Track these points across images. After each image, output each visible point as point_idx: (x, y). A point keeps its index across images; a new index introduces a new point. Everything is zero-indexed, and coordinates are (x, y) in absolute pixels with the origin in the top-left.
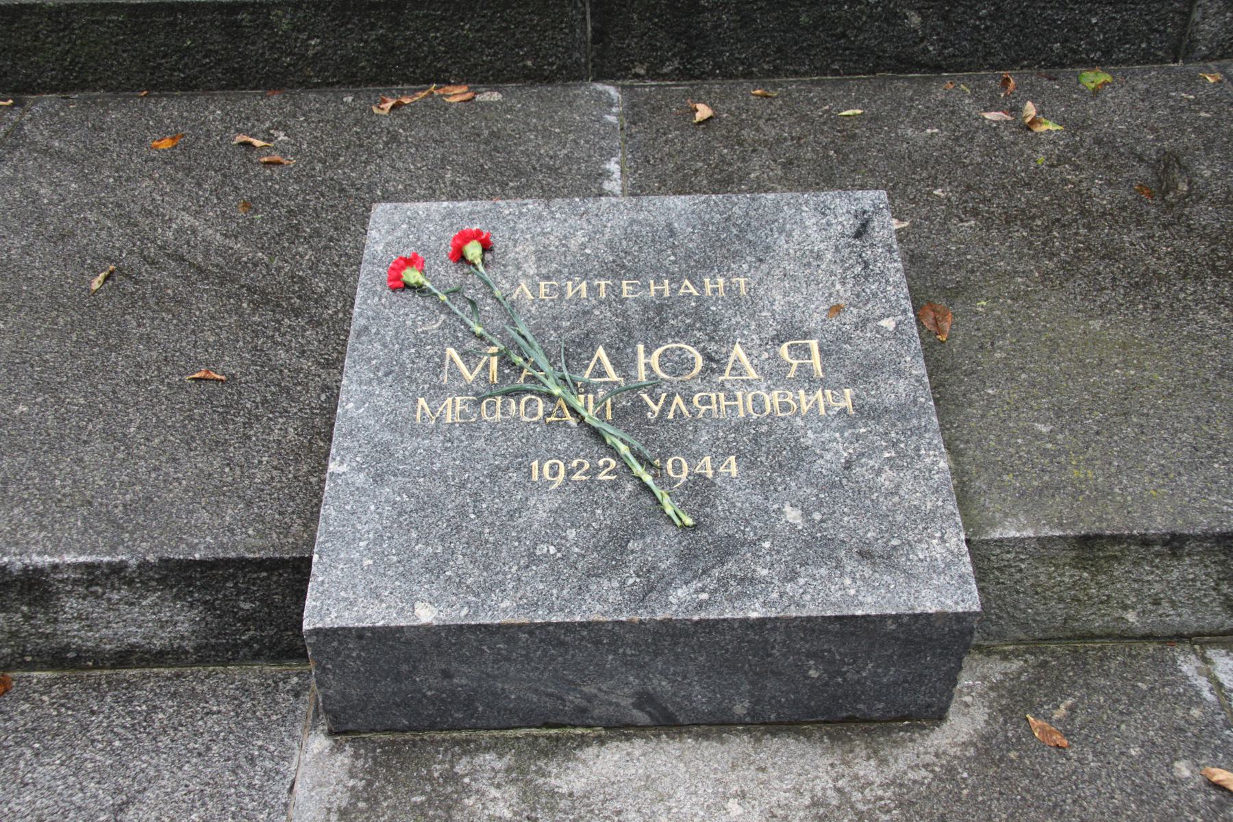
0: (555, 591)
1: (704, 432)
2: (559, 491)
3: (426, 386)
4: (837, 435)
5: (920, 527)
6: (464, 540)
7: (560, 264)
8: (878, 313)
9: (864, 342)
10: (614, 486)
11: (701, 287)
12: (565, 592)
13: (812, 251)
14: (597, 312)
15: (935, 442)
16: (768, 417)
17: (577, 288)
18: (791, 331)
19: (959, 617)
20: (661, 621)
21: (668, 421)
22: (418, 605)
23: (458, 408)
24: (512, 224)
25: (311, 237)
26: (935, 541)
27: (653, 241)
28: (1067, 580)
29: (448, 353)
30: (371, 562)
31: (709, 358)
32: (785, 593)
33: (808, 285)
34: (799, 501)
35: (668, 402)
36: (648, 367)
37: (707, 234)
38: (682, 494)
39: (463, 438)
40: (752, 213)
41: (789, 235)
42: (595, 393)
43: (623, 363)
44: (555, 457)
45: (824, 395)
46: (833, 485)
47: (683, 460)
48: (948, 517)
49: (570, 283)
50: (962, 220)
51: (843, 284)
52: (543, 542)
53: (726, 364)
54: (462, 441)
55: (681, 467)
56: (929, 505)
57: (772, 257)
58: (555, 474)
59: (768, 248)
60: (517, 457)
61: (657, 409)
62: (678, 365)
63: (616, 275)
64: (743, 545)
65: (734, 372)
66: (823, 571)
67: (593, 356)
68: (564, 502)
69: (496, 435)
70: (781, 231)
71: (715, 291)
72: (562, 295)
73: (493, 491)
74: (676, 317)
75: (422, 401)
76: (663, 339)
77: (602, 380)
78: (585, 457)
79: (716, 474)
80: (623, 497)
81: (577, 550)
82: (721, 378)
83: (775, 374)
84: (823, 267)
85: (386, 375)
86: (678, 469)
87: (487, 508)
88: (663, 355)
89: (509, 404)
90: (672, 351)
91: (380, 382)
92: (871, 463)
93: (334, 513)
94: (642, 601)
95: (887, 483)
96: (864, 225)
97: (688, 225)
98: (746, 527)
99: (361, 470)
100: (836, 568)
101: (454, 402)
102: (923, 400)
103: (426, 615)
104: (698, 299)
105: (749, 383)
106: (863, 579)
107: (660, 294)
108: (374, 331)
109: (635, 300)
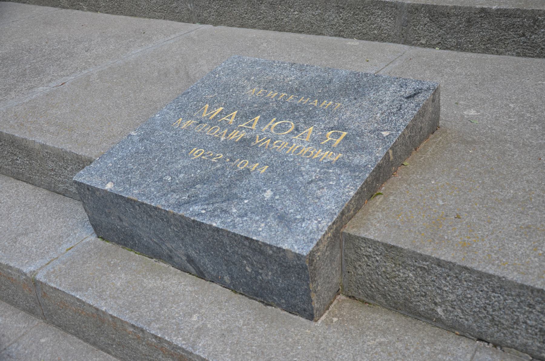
19: (298, 256)
20: (180, 216)
28: (402, 275)
66: (257, 218)
90: (286, 123)
103: (109, 186)
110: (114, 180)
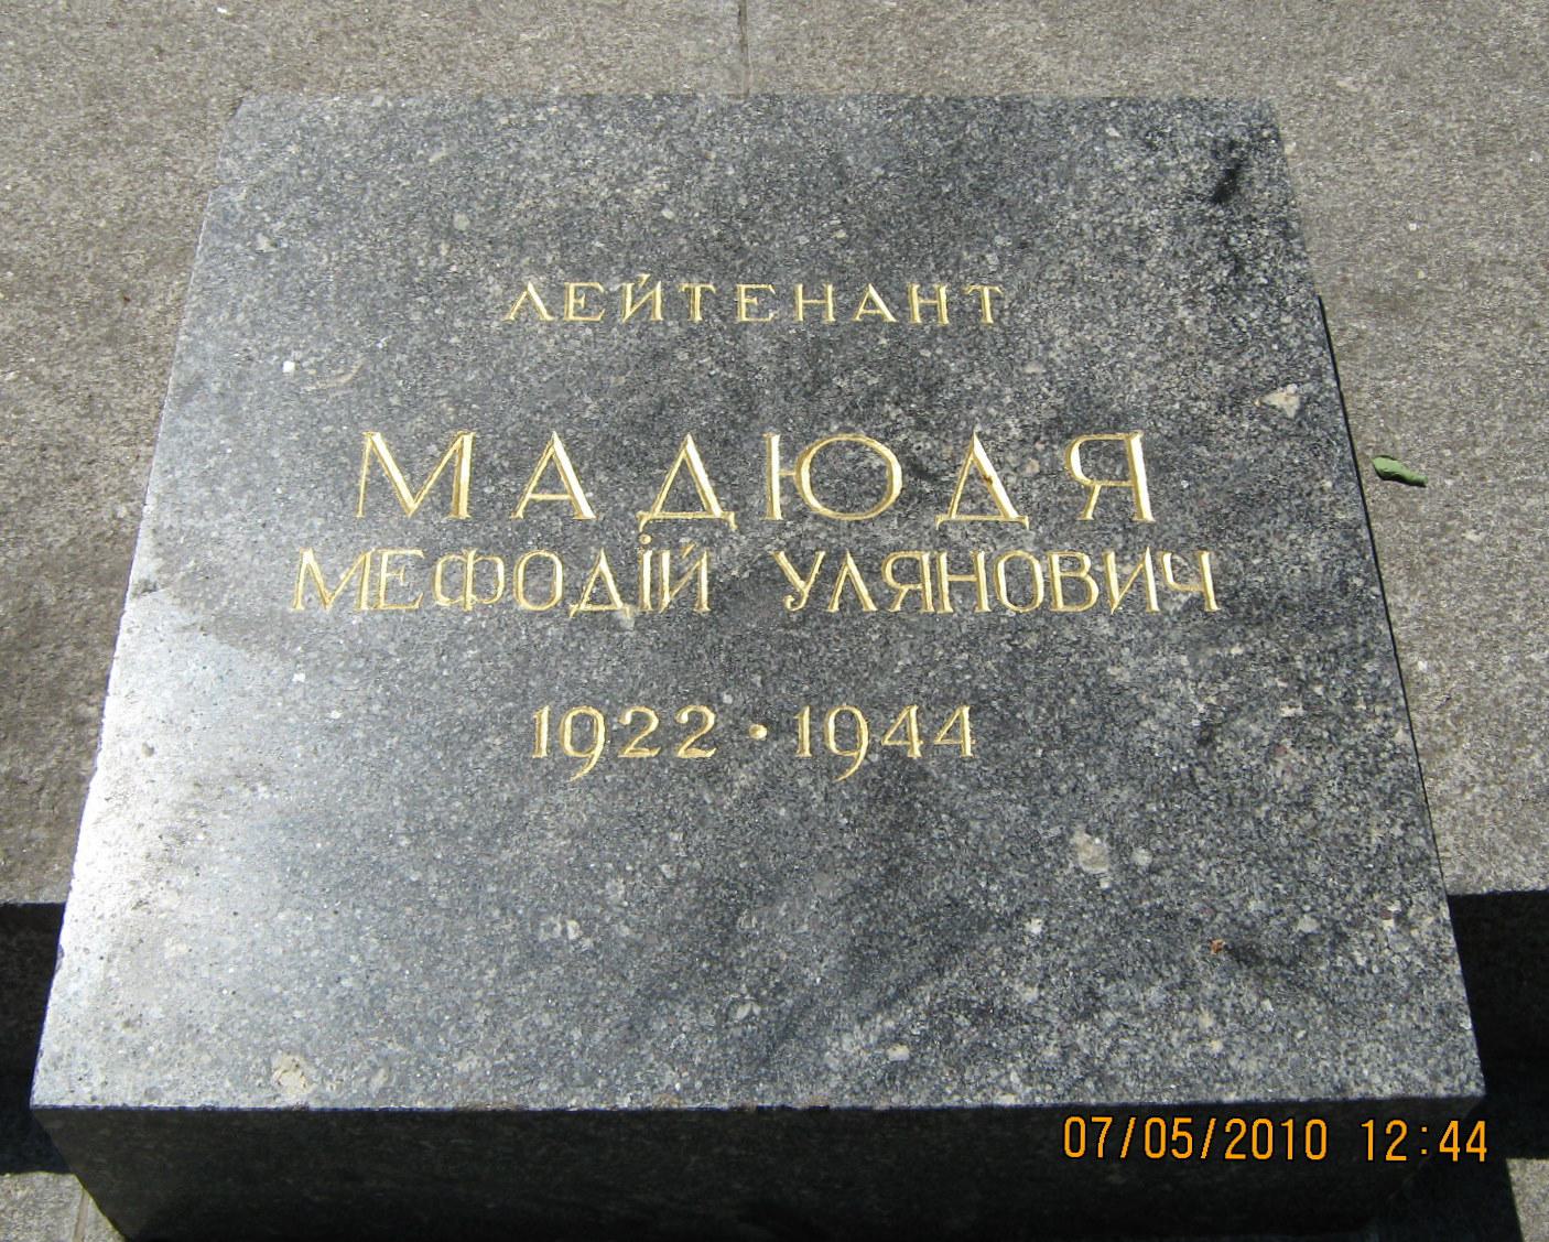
0: (577, 1034)
4: (1184, 660)
5: (1357, 888)
7: (609, 240)
8: (1264, 375)
9: (1236, 446)
10: (710, 773)
11: (901, 306)
12: (598, 1036)
14: (683, 356)
15: (1386, 682)
16: (1038, 613)
17: (640, 297)
18: (1084, 415)
21: (828, 618)
23: (384, 576)
26: (1389, 924)
29: (368, 445)
31: (914, 469)
33: (1121, 306)
34: (1104, 819)
35: (829, 575)
36: (789, 487)
39: (391, 649)
40: (1005, 138)
41: (1082, 190)
42: (675, 547)
43: (738, 483)
45: (1157, 567)
47: (857, 713)
48: (1415, 862)
50: (1393, 147)
51: (1192, 304)
52: (553, 910)
53: (952, 484)
54: (387, 657)
55: (854, 731)
56: (1376, 834)
58: (584, 743)
60: (503, 699)
62: (849, 484)
64: (983, 927)
65: (967, 506)
66: (1155, 995)
67: (671, 460)
71: (929, 312)
75: (308, 557)
76: (819, 420)
77: (690, 516)
78: (648, 703)
81: (626, 931)
82: (941, 518)
83: (1055, 514)
84: (1151, 264)
86: (847, 736)
88: (820, 460)
90: (839, 449)
92: (1255, 729)
94: (765, 1061)
95: (1288, 779)
96: (1233, 174)
97: (874, 162)
98: (990, 881)
100: (1182, 986)
102: (1359, 582)
105: (1000, 531)
106: (1241, 1016)
107: (815, 314)
108: (215, 388)
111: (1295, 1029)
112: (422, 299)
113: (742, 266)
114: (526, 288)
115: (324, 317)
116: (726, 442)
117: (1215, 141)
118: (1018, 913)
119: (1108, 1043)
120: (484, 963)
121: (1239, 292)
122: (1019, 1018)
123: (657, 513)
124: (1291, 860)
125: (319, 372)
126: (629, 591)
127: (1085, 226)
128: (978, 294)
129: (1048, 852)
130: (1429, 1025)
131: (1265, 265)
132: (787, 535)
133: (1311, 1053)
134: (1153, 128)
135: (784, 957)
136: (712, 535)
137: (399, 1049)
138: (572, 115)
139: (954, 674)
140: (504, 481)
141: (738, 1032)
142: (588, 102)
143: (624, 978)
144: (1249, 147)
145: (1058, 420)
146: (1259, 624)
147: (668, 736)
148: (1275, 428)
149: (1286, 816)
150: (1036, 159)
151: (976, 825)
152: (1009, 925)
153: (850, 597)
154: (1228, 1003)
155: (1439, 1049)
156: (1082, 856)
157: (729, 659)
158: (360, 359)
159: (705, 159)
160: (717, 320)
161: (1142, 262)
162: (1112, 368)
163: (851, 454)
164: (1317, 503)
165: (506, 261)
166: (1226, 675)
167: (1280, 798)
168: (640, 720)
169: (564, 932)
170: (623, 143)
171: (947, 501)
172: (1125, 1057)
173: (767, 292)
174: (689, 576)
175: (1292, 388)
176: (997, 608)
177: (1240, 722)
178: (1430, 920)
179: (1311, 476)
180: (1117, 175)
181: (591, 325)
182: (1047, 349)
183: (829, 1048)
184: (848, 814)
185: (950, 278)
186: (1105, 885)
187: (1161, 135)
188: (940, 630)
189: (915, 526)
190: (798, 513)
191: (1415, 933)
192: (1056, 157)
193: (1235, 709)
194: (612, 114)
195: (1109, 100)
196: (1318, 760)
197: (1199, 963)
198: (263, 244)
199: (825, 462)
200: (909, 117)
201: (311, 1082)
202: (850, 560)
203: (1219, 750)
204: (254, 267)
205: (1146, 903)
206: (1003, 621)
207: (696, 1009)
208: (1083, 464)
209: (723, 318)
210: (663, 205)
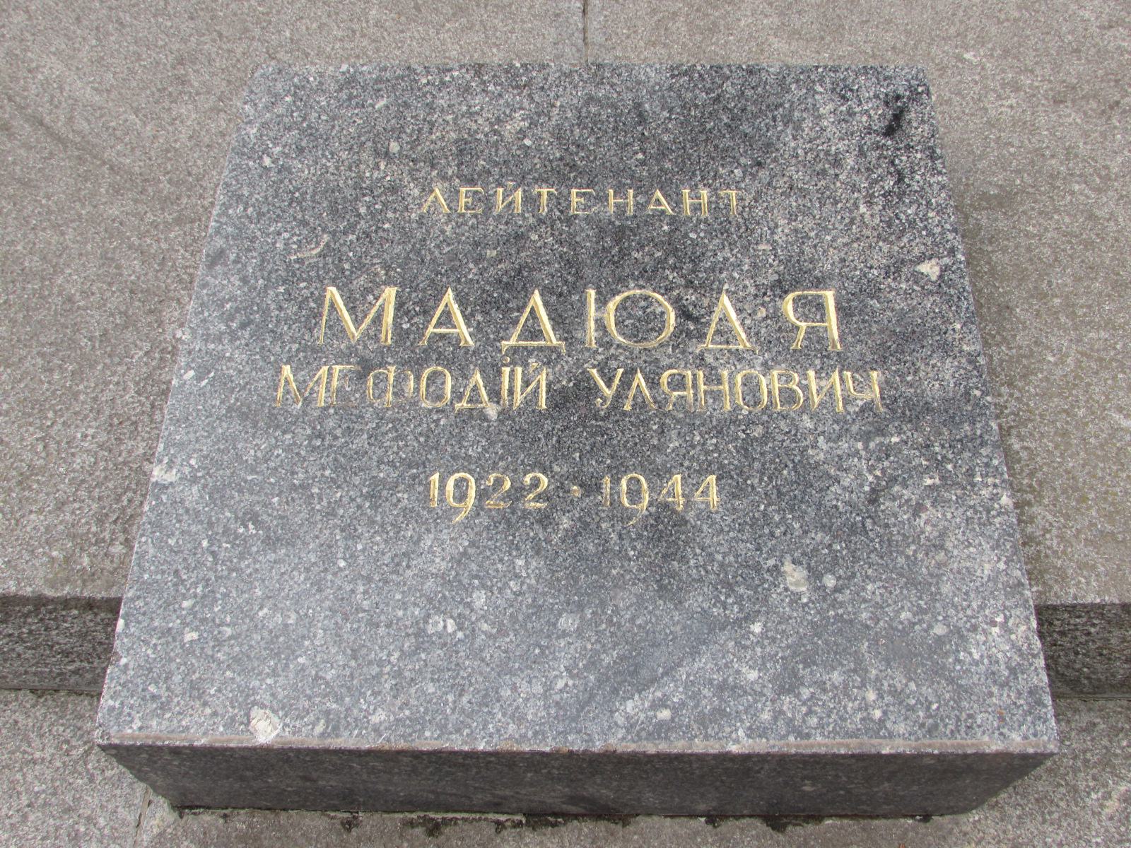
1: (674, 434)
2: (466, 526)
3: (295, 347)
4: (860, 445)
5: (974, 605)
6: (328, 603)
7: (489, 160)
8: (916, 252)
10: (545, 519)
11: (678, 203)
12: (465, 699)
13: (827, 153)
14: (534, 237)
15: (995, 462)
16: (764, 411)
17: (508, 198)
18: (796, 276)
21: (624, 414)
22: (256, 712)
23: (335, 383)
24: (429, 99)
25: (198, 94)
26: (996, 630)
27: (615, 129)
29: (328, 296)
30: (195, 635)
31: (684, 314)
32: (782, 712)
33: (822, 205)
36: (601, 325)
37: (688, 122)
38: (640, 536)
39: (338, 432)
40: (749, 93)
41: (798, 127)
42: (525, 365)
43: (566, 320)
44: (464, 469)
45: (842, 380)
46: (853, 530)
47: (642, 479)
49: (500, 190)
50: (999, 97)
51: (870, 204)
52: (439, 611)
53: (708, 324)
54: (336, 438)
55: (639, 492)
56: (987, 566)
57: (775, 160)
58: (461, 497)
59: (769, 145)
60: (410, 467)
61: (609, 392)
62: (640, 323)
63: (563, 180)
64: (723, 629)
65: (718, 338)
66: (837, 677)
67: (525, 306)
68: (473, 544)
69: (384, 429)
70: (787, 120)
71: (697, 208)
72: (489, 208)
73: (372, 522)
74: (642, 247)
75: (287, 370)
76: (622, 281)
77: (535, 343)
79: (688, 505)
80: (555, 539)
81: (485, 627)
82: (701, 346)
83: (775, 343)
84: (842, 177)
85: (243, 326)
86: (634, 494)
87: (363, 550)
88: (622, 307)
89: (406, 379)
91: (233, 337)
92: (907, 493)
93: (152, 551)
95: (929, 528)
96: (897, 117)
97: (663, 109)
98: (728, 596)
99: (195, 480)
100: (855, 671)
101: (330, 374)
102: (978, 393)
104: (673, 220)
105: (738, 356)
106: (894, 692)
107: (621, 209)
108: (232, 257)
109: (588, 219)
110: (264, 697)
111: (931, 703)
112: (367, 199)
113: (575, 178)
114: (432, 191)
115: (303, 210)
116: (561, 295)
117: (887, 95)
118: (746, 619)
119: (804, 709)
120: (392, 647)
121: (901, 195)
122: (745, 692)
123: (513, 342)
124: (930, 584)
125: (299, 247)
126: (495, 395)
127: (800, 151)
128: (728, 196)
129: (767, 576)
130: (1022, 702)
131: (918, 177)
132: (599, 358)
133: (942, 720)
134: (846, 86)
135: (589, 646)
136: (550, 357)
137: (334, 706)
138: (468, 77)
139: (707, 453)
140: (416, 320)
141: (557, 698)
142: (479, 69)
143: (483, 660)
144: (909, 98)
145: (779, 281)
146: (910, 421)
147: (518, 492)
148: (923, 288)
149: (927, 554)
150: (768, 106)
151: (719, 557)
152: (740, 627)
153: (640, 400)
154: (886, 684)
155: (1029, 719)
156: (789, 579)
157: (558, 442)
158: (326, 238)
159: (553, 106)
160: (558, 213)
161: (837, 175)
162: (815, 246)
163: (643, 303)
164: (950, 339)
165: (423, 174)
166: (888, 456)
167: (923, 541)
168: (498, 482)
169: (445, 627)
170: (500, 95)
171: (705, 335)
172: (816, 720)
173: (590, 194)
174: (533, 385)
175: (934, 261)
176: (737, 409)
177: (896, 488)
178: (1023, 628)
179: (947, 321)
180: (820, 117)
181: (475, 216)
182: (773, 233)
183: (617, 710)
184: (634, 549)
185: (710, 186)
186: (805, 600)
187: (851, 90)
188: (698, 423)
189: (683, 352)
190: (605, 342)
191: (1013, 637)
192: (781, 105)
193: (893, 480)
194: (494, 76)
195: (817, 67)
196: (949, 516)
197: (867, 655)
198: (267, 161)
199: (625, 309)
200: (686, 78)
201: (276, 728)
202: (639, 375)
203: (882, 507)
204: (261, 177)
205: (832, 613)
206: (740, 417)
207: (530, 682)
208: (795, 310)
209: (562, 212)
210: (525, 137)
